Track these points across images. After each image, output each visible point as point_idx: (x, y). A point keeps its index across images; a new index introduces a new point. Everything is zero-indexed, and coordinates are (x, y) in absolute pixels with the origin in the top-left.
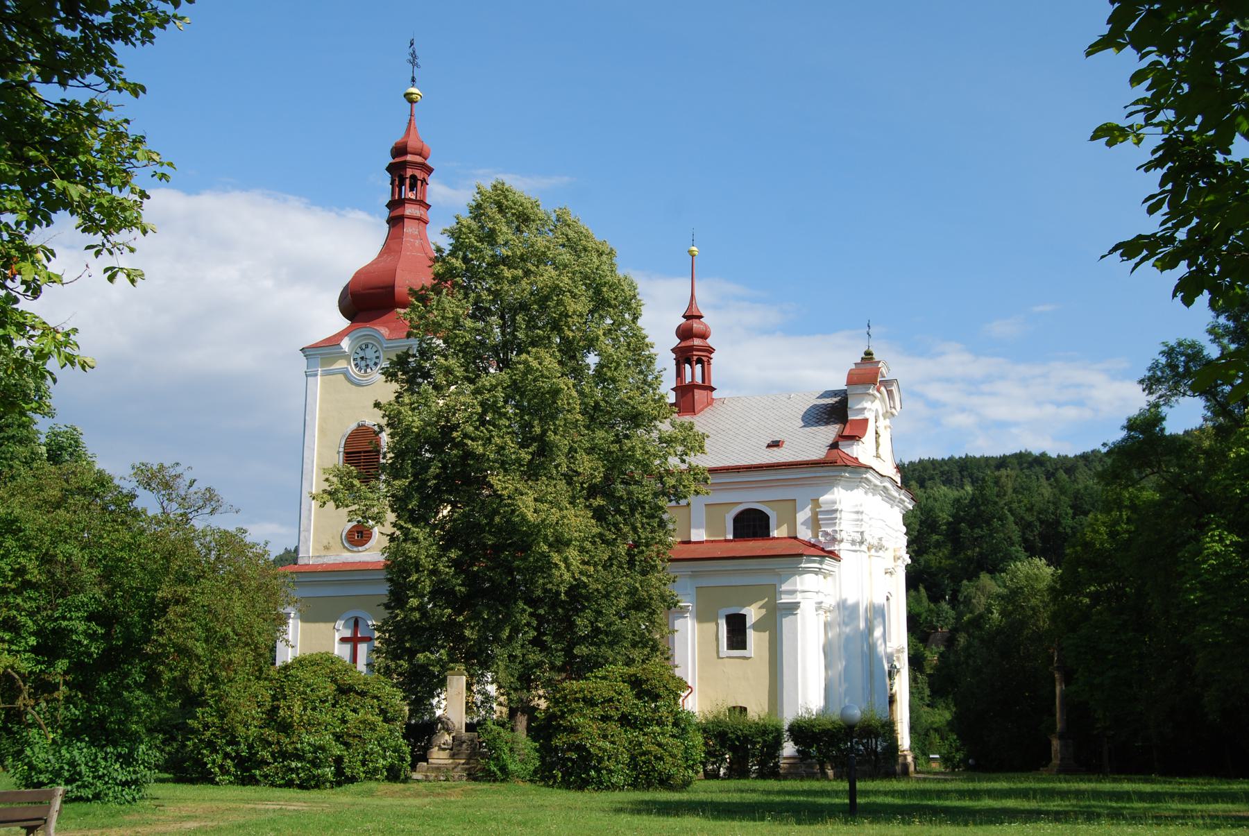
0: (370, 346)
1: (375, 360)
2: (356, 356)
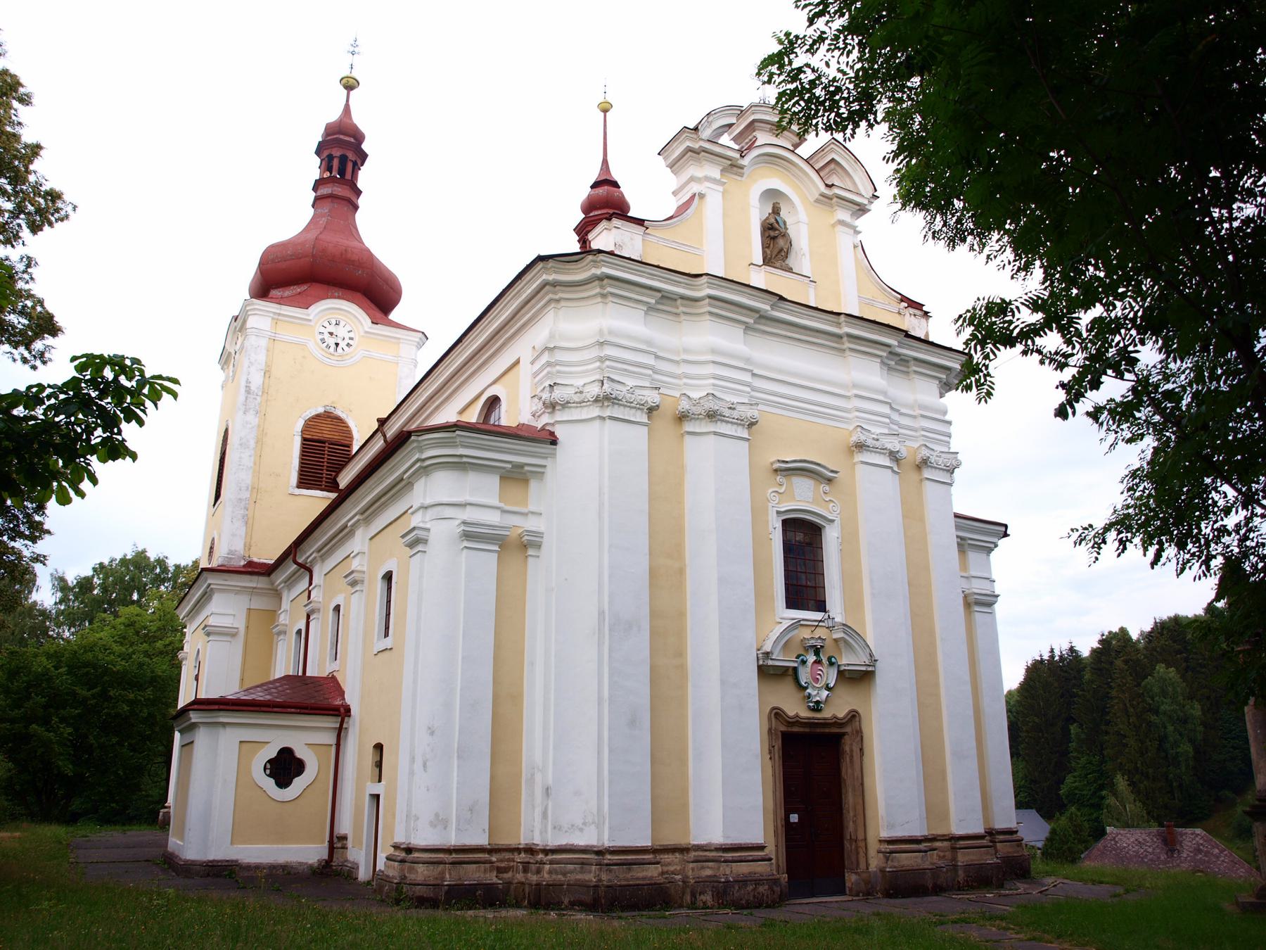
0: (342, 323)
1: (347, 341)
2: (322, 330)
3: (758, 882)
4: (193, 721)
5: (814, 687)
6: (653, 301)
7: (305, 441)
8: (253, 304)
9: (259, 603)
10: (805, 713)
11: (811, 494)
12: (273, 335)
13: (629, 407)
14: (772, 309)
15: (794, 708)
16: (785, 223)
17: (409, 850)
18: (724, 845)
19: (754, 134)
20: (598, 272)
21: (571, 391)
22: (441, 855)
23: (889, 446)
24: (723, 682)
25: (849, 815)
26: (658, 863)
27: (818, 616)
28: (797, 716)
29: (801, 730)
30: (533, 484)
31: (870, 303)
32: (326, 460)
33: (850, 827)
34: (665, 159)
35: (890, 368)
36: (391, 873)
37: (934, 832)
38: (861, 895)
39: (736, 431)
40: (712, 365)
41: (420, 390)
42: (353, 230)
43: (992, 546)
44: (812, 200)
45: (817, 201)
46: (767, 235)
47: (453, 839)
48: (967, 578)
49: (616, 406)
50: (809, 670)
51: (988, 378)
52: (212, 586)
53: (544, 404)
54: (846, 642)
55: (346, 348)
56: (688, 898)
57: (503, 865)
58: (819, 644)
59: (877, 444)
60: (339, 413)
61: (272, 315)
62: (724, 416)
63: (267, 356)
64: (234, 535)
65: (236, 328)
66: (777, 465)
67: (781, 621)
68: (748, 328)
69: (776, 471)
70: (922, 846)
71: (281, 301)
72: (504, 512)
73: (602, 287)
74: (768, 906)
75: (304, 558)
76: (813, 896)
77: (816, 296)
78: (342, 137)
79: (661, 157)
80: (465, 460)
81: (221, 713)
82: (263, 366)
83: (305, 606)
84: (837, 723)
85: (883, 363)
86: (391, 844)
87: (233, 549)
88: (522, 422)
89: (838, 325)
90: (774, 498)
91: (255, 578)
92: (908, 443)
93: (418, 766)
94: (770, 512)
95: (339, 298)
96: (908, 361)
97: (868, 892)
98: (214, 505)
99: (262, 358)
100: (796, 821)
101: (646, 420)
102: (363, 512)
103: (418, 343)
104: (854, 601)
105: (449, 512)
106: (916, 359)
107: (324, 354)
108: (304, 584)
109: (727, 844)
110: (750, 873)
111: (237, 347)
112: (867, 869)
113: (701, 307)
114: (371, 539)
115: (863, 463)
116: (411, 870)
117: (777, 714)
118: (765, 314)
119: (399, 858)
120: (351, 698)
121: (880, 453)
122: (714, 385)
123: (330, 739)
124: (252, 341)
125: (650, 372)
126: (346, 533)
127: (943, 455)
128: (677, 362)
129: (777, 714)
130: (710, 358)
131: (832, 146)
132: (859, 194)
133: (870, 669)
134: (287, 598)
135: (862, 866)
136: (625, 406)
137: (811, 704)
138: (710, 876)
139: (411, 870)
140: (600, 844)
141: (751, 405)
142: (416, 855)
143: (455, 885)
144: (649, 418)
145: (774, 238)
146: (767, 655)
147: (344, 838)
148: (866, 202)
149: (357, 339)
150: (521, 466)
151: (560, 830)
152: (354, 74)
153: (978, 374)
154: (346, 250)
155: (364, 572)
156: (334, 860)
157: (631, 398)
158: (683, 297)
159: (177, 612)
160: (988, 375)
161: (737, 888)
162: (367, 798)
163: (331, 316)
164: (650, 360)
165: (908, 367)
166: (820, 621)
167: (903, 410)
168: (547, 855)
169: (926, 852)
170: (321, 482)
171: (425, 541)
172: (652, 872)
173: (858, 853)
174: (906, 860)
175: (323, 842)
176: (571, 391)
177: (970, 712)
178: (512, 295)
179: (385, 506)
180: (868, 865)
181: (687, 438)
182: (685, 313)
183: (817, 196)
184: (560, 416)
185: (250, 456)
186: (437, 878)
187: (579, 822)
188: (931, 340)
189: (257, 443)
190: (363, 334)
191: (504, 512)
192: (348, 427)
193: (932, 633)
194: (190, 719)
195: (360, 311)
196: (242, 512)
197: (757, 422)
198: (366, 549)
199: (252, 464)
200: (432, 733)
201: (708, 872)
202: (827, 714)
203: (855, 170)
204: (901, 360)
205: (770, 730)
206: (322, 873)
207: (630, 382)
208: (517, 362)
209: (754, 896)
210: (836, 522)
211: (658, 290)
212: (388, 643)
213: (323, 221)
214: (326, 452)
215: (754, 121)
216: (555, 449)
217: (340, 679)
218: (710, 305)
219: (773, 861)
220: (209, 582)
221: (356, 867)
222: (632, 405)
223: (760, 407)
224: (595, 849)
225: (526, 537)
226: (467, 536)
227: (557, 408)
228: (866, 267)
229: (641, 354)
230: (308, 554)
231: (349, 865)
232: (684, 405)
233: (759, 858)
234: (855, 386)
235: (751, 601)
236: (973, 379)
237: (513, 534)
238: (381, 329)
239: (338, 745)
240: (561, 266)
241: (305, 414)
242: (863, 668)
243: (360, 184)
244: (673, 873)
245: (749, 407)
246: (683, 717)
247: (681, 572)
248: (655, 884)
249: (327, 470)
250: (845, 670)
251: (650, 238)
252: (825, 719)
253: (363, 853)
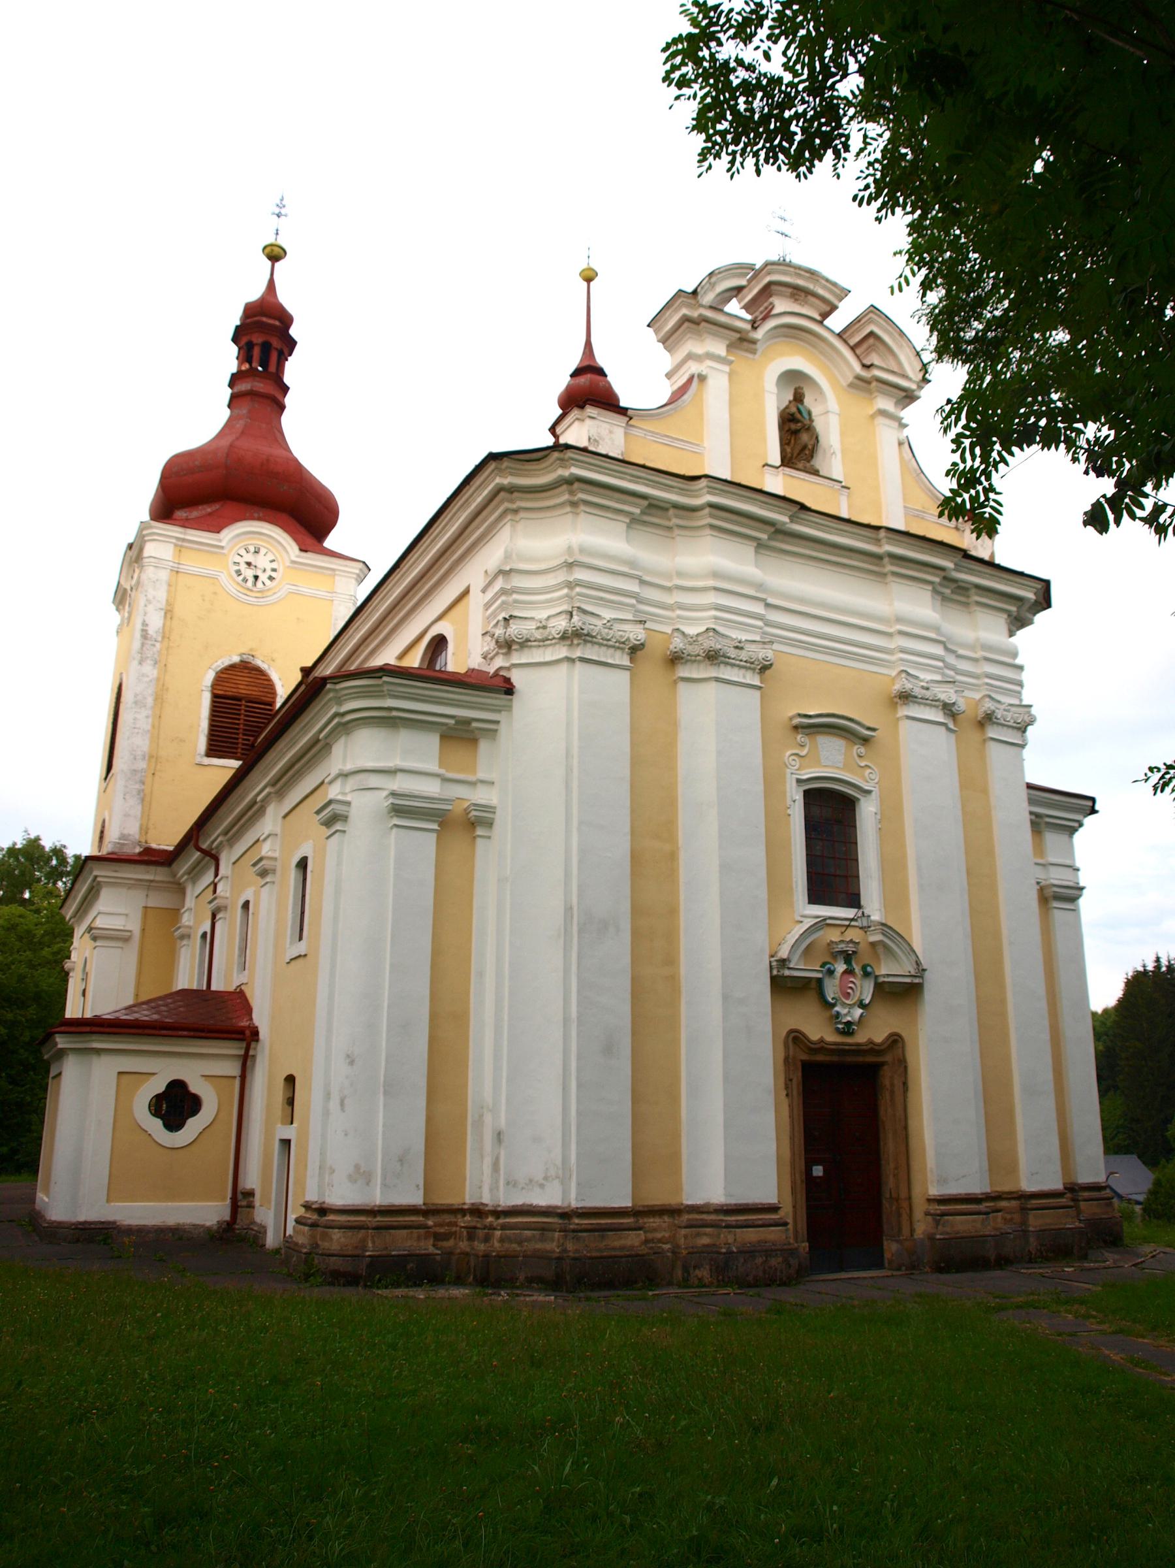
0: (263, 551)
1: (269, 573)
2: (237, 559)
3: (768, 1251)
4: (60, 1046)
5: (844, 1005)
6: (637, 511)
7: (216, 697)
8: (151, 527)
9: (158, 900)
10: (831, 1037)
11: (841, 758)
12: (176, 565)
13: (606, 645)
14: (792, 521)
15: (817, 1030)
16: (810, 413)
17: (323, 1211)
18: (727, 1205)
19: (771, 300)
20: (565, 473)
21: (532, 625)
22: (362, 1218)
23: (942, 697)
24: (725, 998)
25: (888, 1167)
26: (640, 1229)
27: (849, 913)
28: (822, 1040)
29: (828, 1058)
30: (484, 745)
31: (918, 515)
32: (242, 721)
33: (889, 1183)
34: (656, 332)
35: (945, 599)
36: (301, 1240)
37: (999, 1189)
38: (904, 1268)
39: (744, 677)
40: (712, 594)
41: (351, 631)
42: (278, 434)
43: (1076, 825)
44: (845, 384)
45: (851, 385)
46: (786, 428)
47: (378, 1197)
48: (1043, 865)
49: (589, 645)
50: (837, 982)
51: (992, 495)
52: (99, 879)
53: (497, 642)
54: (885, 946)
55: (268, 582)
56: (679, 1272)
57: (442, 1230)
58: (850, 948)
59: (928, 694)
60: (259, 663)
61: (174, 541)
62: (729, 658)
63: (169, 592)
64: (127, 815)
65: (131, 558)
66: (797, 721)
67: (801, 919)
68: (760, 546)
69: (796, 728)
70: (982, 1207)
71: (185, 524)
72: (445, 780)
73: (572, 493)
74: (783, 1284)
75: (208, 842)
76: (841, 1269)
77: (850, 507)
78: (264, 319)
79: (650, 330)
80: (395, 714)
81: (94, 1037)
82: (163, 604)
83: (210, 902)
84: (872, 1049)
85: (935, 591)
86: (302, 1202)
87: (126, 832)
88: (472, 667)
89: (878, 541)
90: (793, 763)
91: (152, 868)
92: (967, 693)
93: (334, 1105)
94: (788, 780)
95: (259, 519)
96: (967, 589)
97: (911, 1265)
98: (106, 778)
99: (161, 595)
100: (821, 1174)
101: (628, 663)
102: (274, 783)
103: (358, 575)
104: (896, 896)
105: (374, 781)
106: (978, 587)
107: (239, 588)
108: (209, 877)
109: (730, 1205)
110: (759, 1242)
111: (134, 582)
112: (912, 1235)
113: (702, 518)
114: (285, 817)
115: (908, 717)
116: (325, 1236)
117: (796, 1038)
118: (783, 528)
119: (309, 1221)
120: (261, 1018)
121: (931, 706)
122: (716, 618)
123: (233, 1069)
124: (149, 573)
125: (633, 601)
126: (255, 811)
127: (1013, 709)
128: (668, 589)
129: (796, 1038)
130: (711, 583)
131: (871, 315)
132: (905, 376)
133: (917, 981)
134: (191, 892)
135: (906, 1231)
136: (600, 645)
137: (840, 1026)
138: (704, 1246)
139: (325, 1236)
140: (565, 1205)
141: (764, 643)
142: (331, 1217)
143: (379, 1256)
144: (632, 660)
145: (795, 433)
146: (783, 962)
147: (250, 1194)
148: (914, 387)
149: (281, 569)
150: (467, 722)
151: (515, 1185)
152: (281, 242)
153: (974, 488)
154: (268, 460)
155: (275, 859)
156: (238, 1221)
157: (608, 634)
158: (677, 506)
159: (63, 911)
160: (991, 489)
161: (742, 1260)
162: (277, 1145)
163: (250, 542)
164: (633, 587)
165: (968, 597)
166: (852, 920)
167: (961, 652)
168: (498, 1218)
169: (987, 1213)
170: (237, 748)
171: (344, 818)
172: (633, 1240)
173: (899, 1215)
174: (962, 1224)
175: (224, 1199)
176: (532, 625)
177: (1046, 1036)
178: (459, 504)
179: (299, 775)
180: (912, 1231)
181: (682, 686)
182: (680, 527)
183: (851, 379)
184: (516, 658)
185: (147, 717)
186: (356, 1247)
187: (539, 1177)
188: (997, 561)
189: (156, 700)
190: (288, 564)
191: (445, 780)
192: (270, 680)
193: (997, 935)
194: (56, 1044)
195: (285, 535)
196: (137, 786)
197: (771, 665)
198: (278, 830)
199: (149, 727)
200: (352, 1063)
201: (705, 1241)
202: (861, 1038)
203: (901, 347)
204: (959, 587)
205: (786, 1060)
206: (221, 1239)
207: (607, 614)
208: (466, 592)
209: (764, 1271)
210: (874, 793)
211: (643, 497)
212: (301, 948)
213: (240, 425)
214: (243, 712)
215: (770, 284)
216: (511, 700)
217: (248, 995)
218: (711, 516)
219: (790, 1226)
220: (95, 873)
221: (263, 1230)
222: (610, 643)
223: (776, 646)
224: (559, 1211)
225: (474, 813)
226: (397, 811)
227: (514, 647)
228: (915, 471)
229: (621, 578)
230: (213, 838)
231: (256, 1228)
232: (678, 643)
233: (772, 1222)
234: (899, 620)
235: (763, 893)
236: (966, 496)
237: (458, 808)
238: (311, 559)
239: (243, 1077)
240: (518, 466)
241: (216, 664)
242: (908, 980)
243: (287, 379)
244: (660, 1241)
245: (761, 646)
246: (676, 1041)
247: (673, 856)
248: (637, 1255)
249: (244, 735)
250: (884, 982)
251: (634, 431)
252: (858, 1045)
253: (271, 1214)
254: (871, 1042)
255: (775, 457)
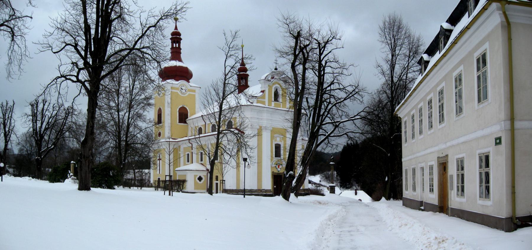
7: (179, 113)
10: (277, 172)
15: (276, 171)
27: (280, 158)
60: (185, 106)
129: (273, 172)
202: (280, 172)
254: (281, 173)
255: (273, 100)
